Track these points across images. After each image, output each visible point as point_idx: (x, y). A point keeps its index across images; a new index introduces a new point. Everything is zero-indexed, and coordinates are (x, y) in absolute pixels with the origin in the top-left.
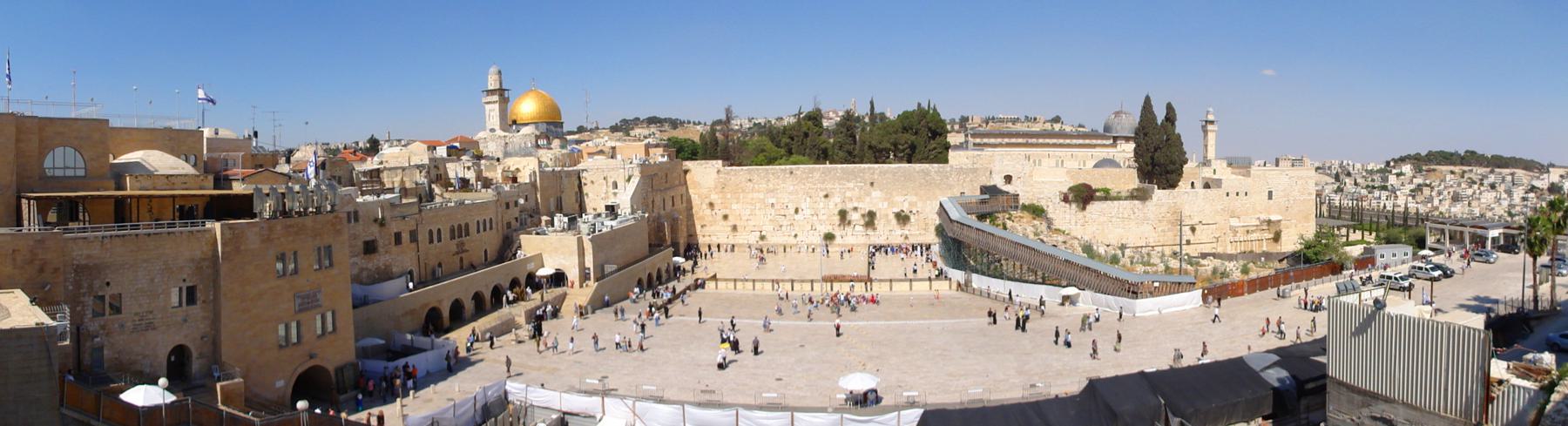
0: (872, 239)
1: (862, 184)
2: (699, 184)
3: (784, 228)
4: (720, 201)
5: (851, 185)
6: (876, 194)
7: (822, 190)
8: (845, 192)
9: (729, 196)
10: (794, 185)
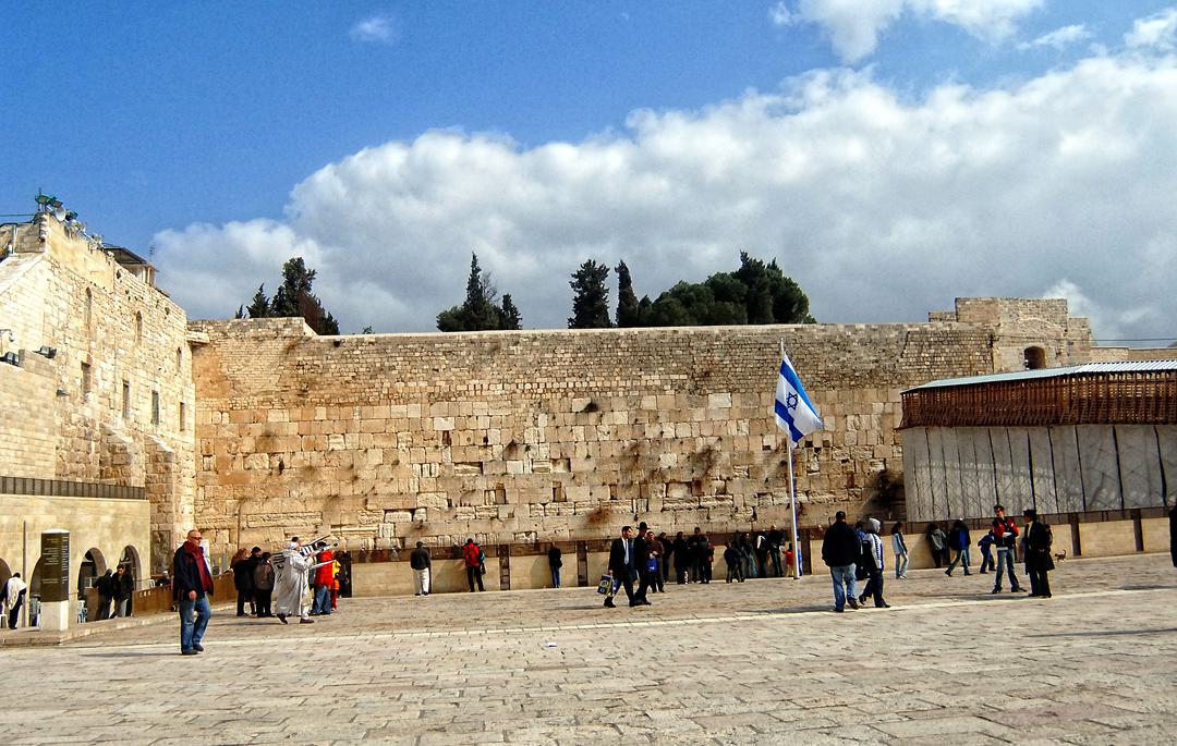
0: (715, 518)
1: (686, 377)
2: (235, 382)
3: (478, 500)
4: (293, 429)
5: (655, 379)
6: (719, 400)
7: (578, 393)
8: (640, 398)
9: (321, 413)
10: (503, 382)
